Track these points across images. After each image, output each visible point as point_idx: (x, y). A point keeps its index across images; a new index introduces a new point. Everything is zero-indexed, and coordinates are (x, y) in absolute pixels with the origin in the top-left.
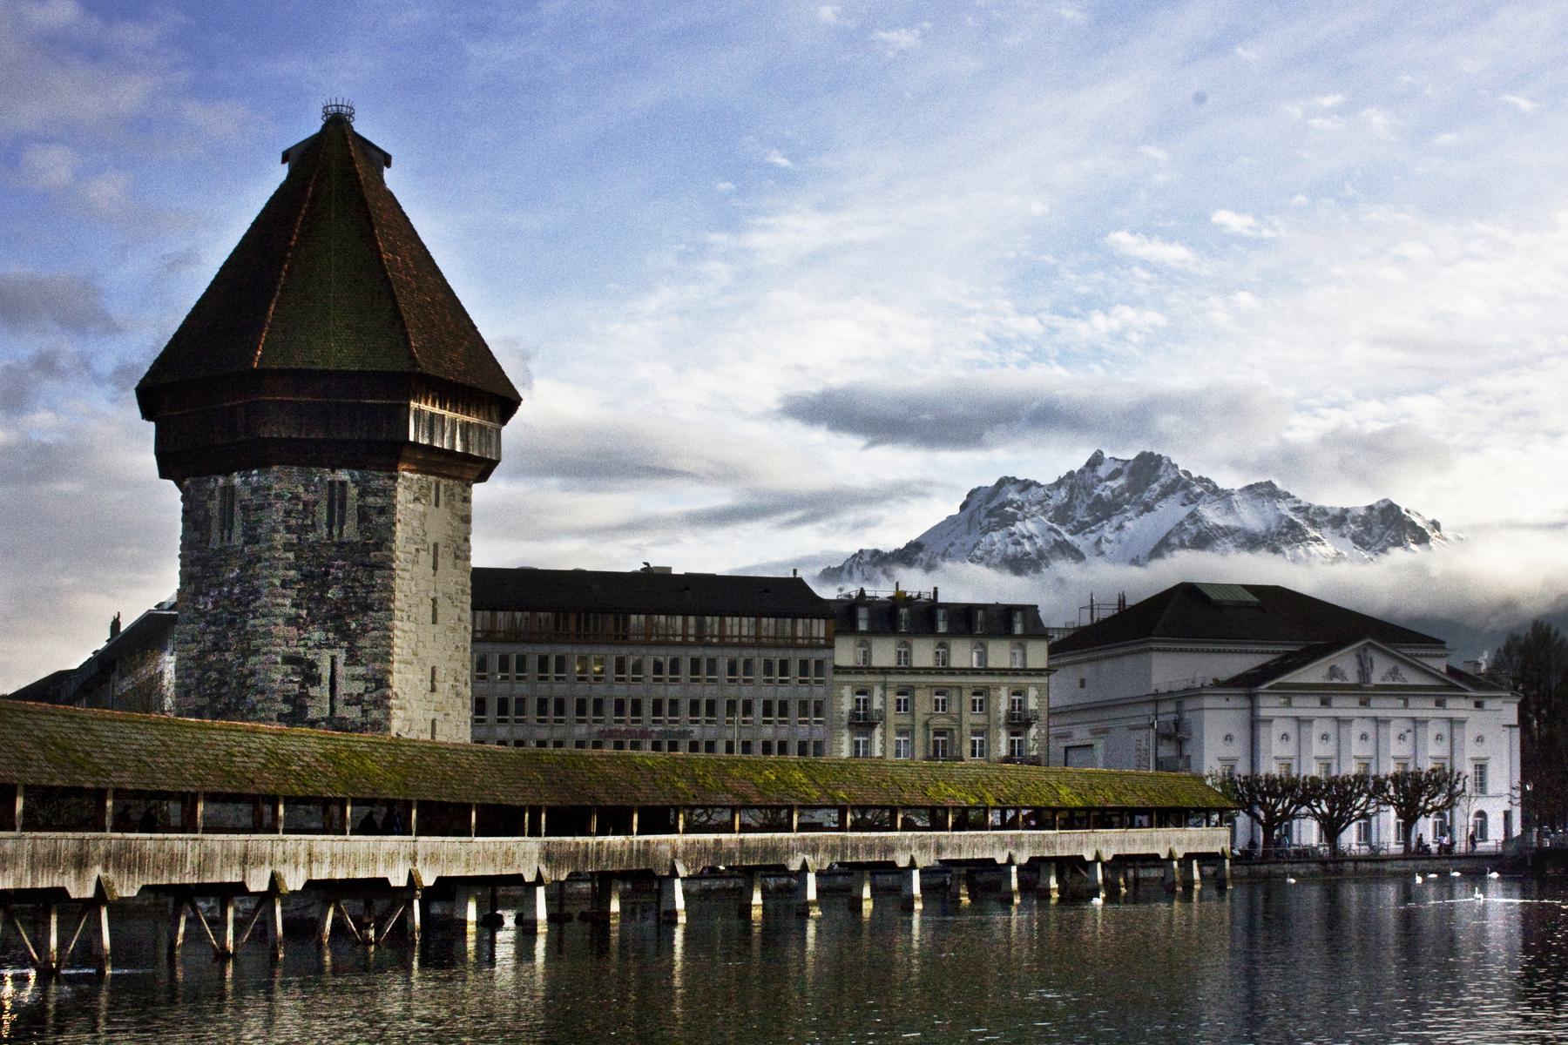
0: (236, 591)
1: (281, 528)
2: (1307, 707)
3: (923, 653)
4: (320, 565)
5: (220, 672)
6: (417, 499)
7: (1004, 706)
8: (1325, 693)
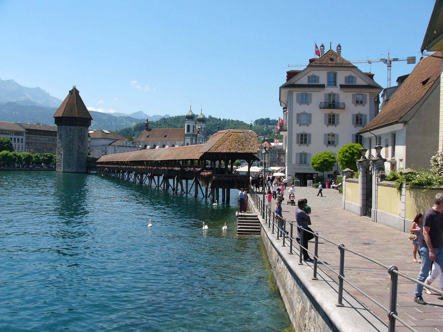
2: (120, 148)
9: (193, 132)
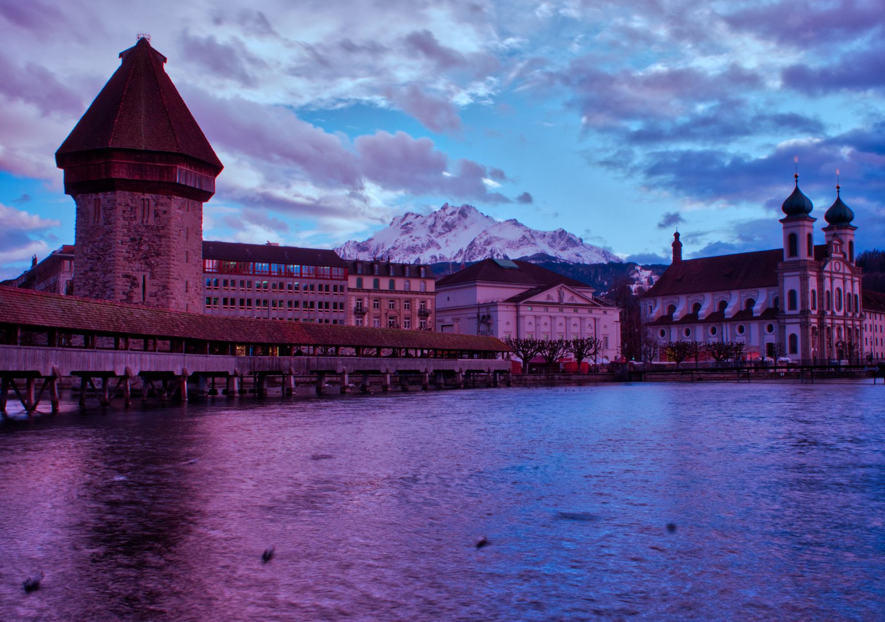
1: (121, 218)
2: (539, 311)
3: (384, 284)
4: (139, 235)
5: (95, 280)
6: (180, 208)
7: (418, 307)
8: (546, 305)
9: (809, 254)
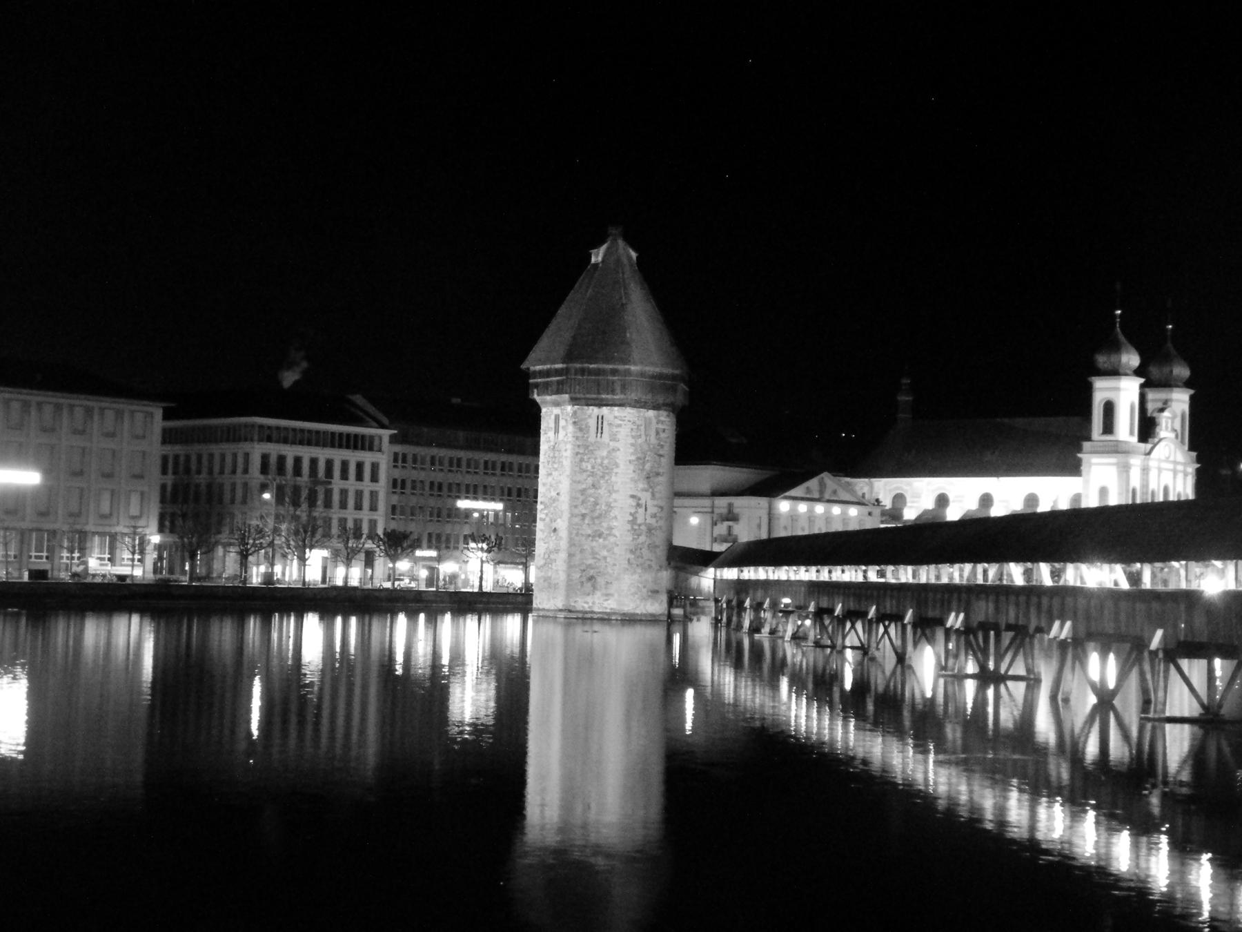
0: (606, 462)
9: (1132, 433)
